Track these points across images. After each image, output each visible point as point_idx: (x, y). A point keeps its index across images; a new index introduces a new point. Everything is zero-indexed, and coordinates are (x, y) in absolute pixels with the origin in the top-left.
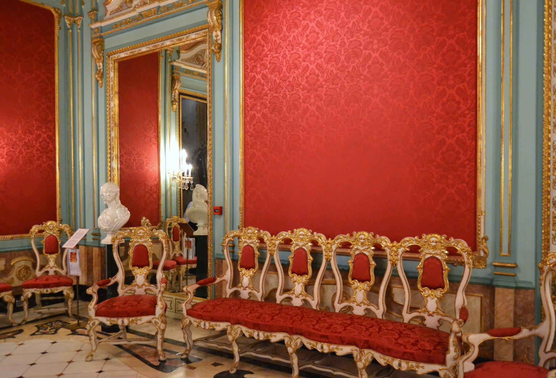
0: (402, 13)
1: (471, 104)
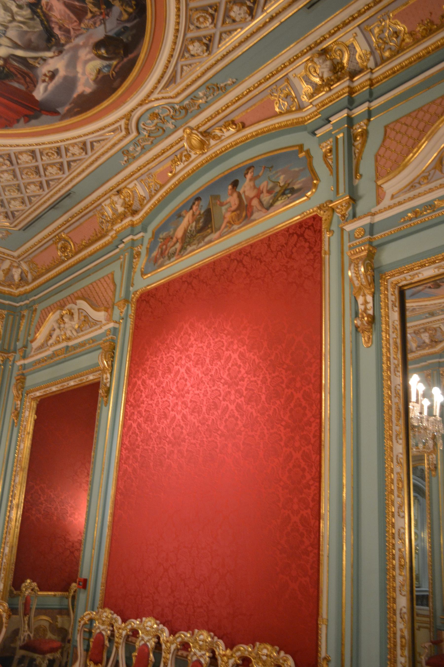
0: (257, 361)
1: (315, 472)
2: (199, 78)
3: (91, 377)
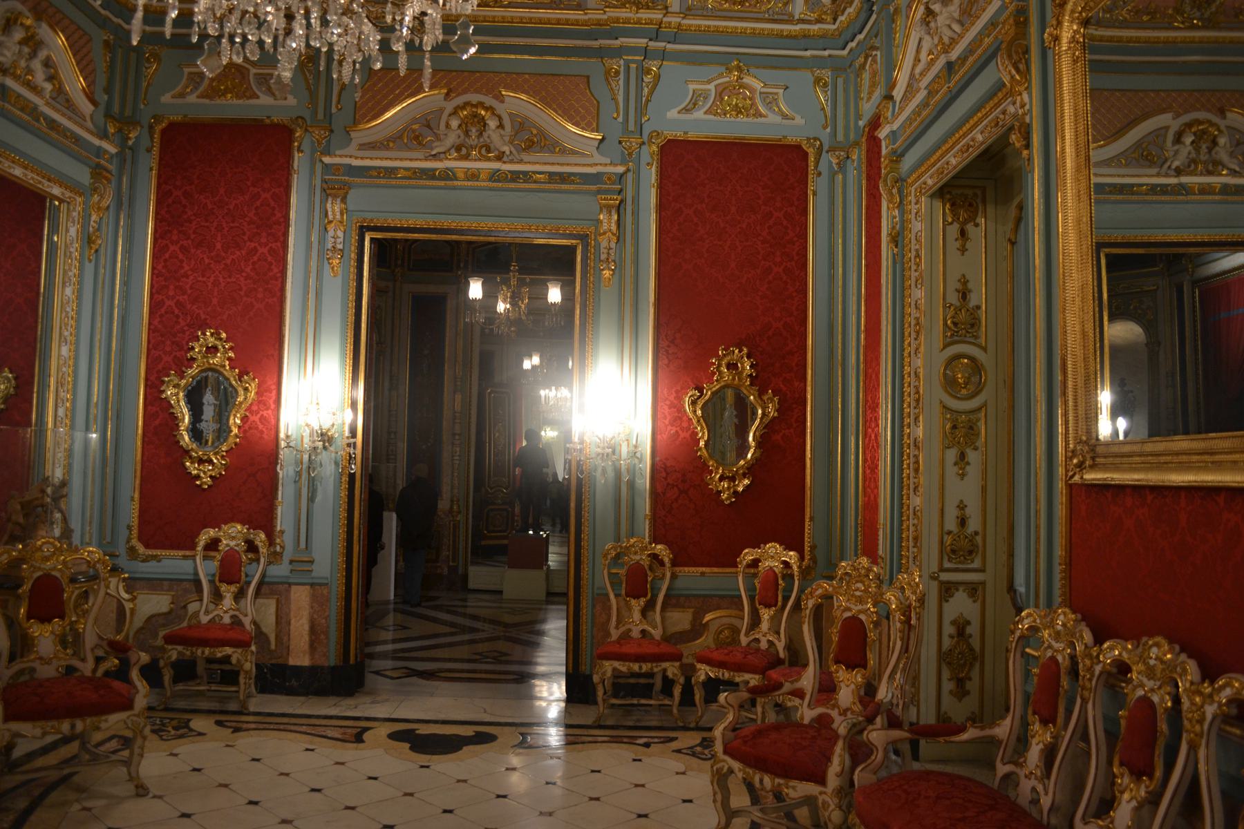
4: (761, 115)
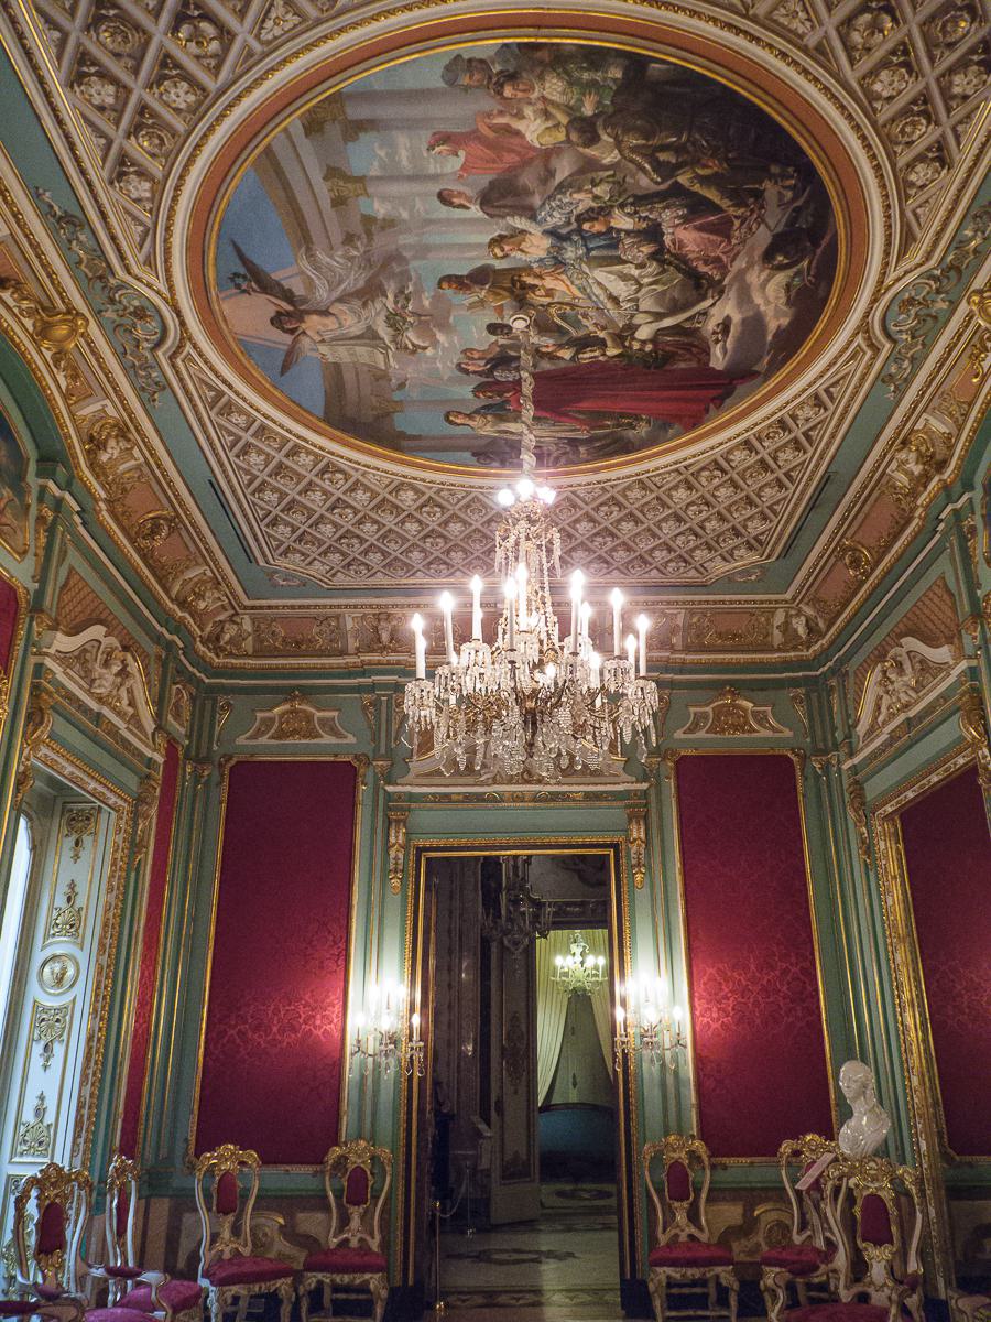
2: (951, 212)
3: (961, 761)
4: (755, 731)
